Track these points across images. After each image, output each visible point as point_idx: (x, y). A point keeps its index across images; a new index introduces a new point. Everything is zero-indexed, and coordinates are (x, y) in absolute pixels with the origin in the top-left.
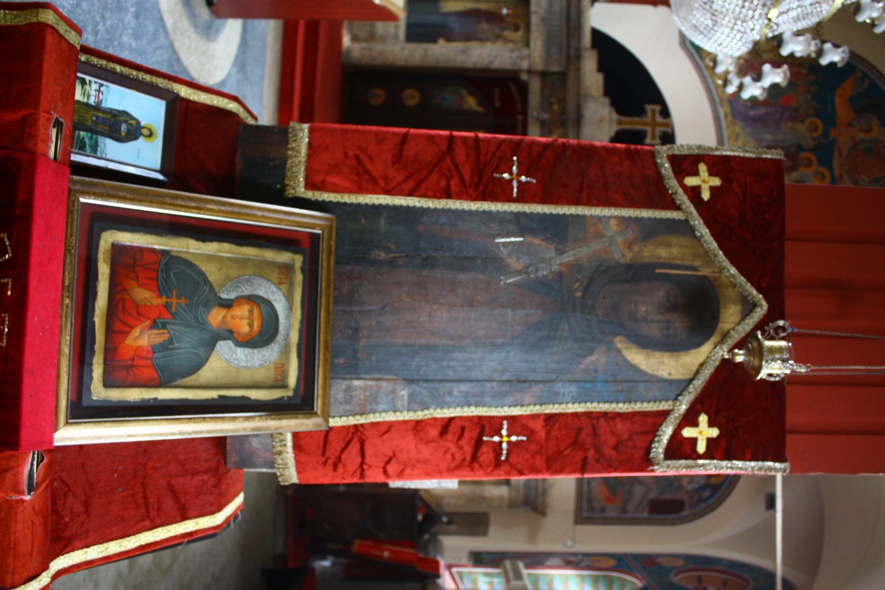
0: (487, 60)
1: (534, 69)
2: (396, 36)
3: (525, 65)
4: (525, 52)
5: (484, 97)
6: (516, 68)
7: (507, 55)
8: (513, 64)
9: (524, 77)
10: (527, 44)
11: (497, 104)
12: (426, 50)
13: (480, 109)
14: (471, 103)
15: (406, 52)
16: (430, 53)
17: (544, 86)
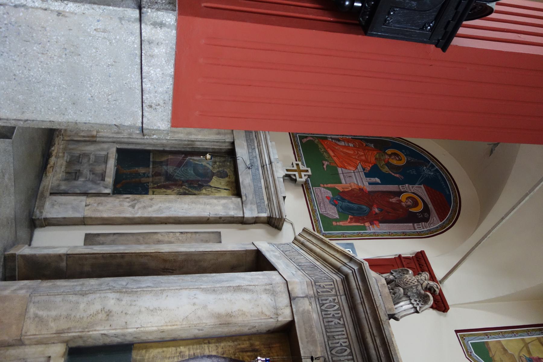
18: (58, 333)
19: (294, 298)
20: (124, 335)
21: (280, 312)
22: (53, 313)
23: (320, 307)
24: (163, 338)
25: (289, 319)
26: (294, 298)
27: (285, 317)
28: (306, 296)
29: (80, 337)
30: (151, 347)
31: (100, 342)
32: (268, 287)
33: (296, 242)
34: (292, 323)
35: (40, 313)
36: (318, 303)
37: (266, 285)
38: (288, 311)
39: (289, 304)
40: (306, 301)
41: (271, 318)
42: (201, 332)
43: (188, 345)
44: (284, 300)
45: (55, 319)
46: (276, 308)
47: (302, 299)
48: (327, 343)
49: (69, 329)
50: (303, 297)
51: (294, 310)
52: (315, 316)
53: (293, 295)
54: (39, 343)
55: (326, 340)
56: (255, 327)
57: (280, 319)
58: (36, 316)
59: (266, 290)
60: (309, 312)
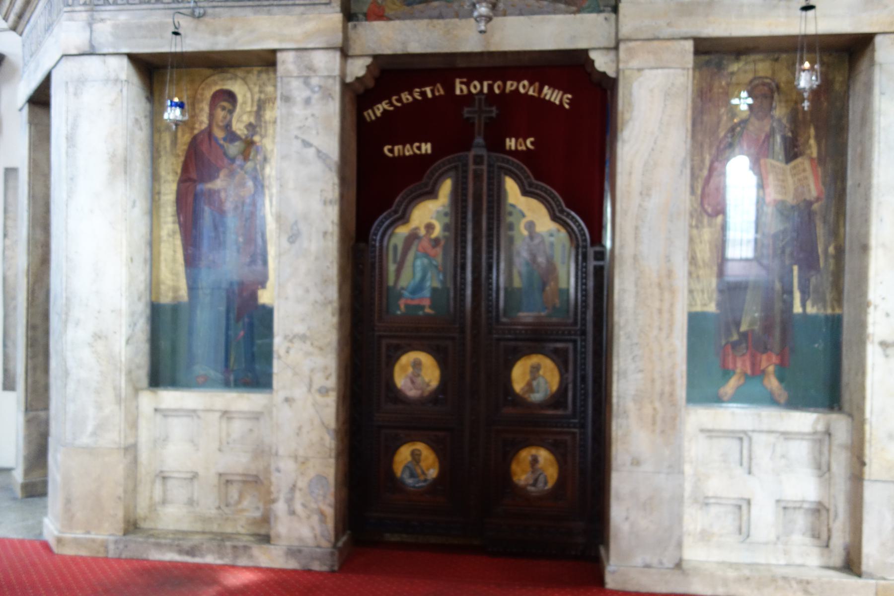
0: (317, 168)
1: (338, 40)
2: (256, 416)
3: (327, 63)
4: (287, 62)
5: (415, 180)
6: (337, 89)
7: (298, 111)
8: (326, 95)
9: (358, 68)
10: (267, 61)
11: (427, 148)
12: (291, 339)
13: (446, 187)
14: (430, 214)
15: (299, 392)
16: (300, 329)
17: (378, 14)
18: (119, 400)
19: (92, 46)
20: (132, 314)
21: (113, 76)
22: (91, 411)
23: (110, 4)
24: (145, 260)
25: (125, 61)
26: (92, 46)
27: (123, 68)
28: (90, 25)
29: (129, 373)
30: (158, 277)
31: (145, 347)
32: (71, 90)
33: (20, 29)
34: (134, 59)
35: (90, 428)
36: (103, 8)
37: (67, 92)
38: (113, 61)
39: (102, 57)
40: (98, 26)
41: (121, 91)
42: (138, 204)
43: (159, 225)
44: (93, 62)
45: (99, 407)
46: (107, 80)
47: (94, 35)
48: (167, 6)
49: (115, 388)
50: (91, 31)
51: (111, 51)
52: (123, 17)
53: (87, 49)
54: (133, 425)
55: (161, 6)
56: (137, 120)
57: (123, 76)
58: (94, 434)
59: (75, 94)
60: (116, 27)
